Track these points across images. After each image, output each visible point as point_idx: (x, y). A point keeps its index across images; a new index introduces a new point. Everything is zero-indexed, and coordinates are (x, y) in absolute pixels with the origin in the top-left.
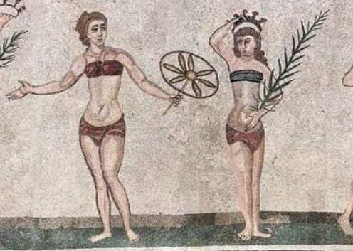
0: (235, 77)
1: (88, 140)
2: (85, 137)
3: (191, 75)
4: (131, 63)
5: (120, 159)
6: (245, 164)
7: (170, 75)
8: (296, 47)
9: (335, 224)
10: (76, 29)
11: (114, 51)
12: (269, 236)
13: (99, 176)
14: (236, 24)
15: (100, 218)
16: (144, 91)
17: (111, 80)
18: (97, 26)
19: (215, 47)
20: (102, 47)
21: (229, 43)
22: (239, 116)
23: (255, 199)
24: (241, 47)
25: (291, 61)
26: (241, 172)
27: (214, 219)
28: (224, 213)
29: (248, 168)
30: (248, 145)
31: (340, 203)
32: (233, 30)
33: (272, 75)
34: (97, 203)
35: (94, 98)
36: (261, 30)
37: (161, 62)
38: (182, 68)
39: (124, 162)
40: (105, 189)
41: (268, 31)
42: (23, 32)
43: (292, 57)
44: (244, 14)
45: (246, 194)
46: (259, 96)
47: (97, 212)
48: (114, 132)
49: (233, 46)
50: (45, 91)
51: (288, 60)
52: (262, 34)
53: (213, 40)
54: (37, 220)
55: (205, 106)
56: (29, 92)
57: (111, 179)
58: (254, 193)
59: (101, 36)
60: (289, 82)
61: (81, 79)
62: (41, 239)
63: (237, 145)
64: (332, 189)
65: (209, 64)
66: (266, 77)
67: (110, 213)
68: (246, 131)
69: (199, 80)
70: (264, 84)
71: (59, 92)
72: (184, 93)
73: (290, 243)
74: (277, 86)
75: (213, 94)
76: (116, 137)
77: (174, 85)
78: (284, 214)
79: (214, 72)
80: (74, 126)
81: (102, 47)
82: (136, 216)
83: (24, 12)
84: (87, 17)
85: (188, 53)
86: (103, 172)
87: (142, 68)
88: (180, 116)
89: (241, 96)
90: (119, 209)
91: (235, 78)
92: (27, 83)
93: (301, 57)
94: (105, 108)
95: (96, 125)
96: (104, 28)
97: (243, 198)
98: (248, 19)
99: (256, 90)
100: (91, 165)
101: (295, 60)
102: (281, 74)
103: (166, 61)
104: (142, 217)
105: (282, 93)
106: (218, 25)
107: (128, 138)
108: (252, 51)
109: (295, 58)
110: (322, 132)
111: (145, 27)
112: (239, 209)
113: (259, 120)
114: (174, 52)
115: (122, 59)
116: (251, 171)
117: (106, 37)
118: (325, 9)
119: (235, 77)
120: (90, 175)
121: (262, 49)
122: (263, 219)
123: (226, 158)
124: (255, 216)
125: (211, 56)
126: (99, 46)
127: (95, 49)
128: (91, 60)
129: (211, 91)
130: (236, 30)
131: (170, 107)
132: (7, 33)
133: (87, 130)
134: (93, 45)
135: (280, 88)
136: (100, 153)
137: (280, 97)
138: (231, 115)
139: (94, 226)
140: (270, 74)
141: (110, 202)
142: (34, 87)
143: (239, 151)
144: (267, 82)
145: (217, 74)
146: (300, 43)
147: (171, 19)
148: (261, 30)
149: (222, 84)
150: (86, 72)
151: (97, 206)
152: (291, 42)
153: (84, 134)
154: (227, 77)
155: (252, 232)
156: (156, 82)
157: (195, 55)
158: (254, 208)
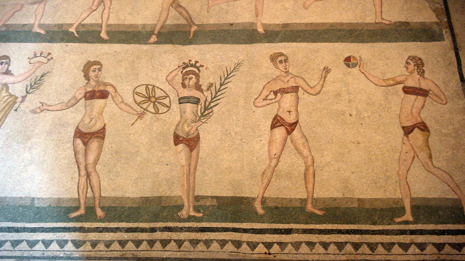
0: (182, 100)
1: (79, 141)
2: (78, 139)
3: (153, 99)
4: (114, 91)
5: (99, 155)
6: (185, 160)
7: (139, 99)
8: (222, 82)
9: (250, 207)
10: (82, 71)
11: (106, 84)
12: (201, 215)
13: (82, 167)
14: (184, 68)
15: (79, 199)
16: (121, 109)
17: (102, 101)
18: (96, 69)
19: (170, 82)
20: (97, 82)
21: (179, 79)
22: (183, 125)
23: (191, 186)
24: (186, 82)
25: (219, 91)
26: (183, 166)
27: (161, 202)
28: (168, 196)
29: (187, 163)
30: (189, 146)
31: (253, 189)
32: (182, 72)
33: (206, 100)
34: (78, 187)
35: (87, 114)
36: (200, 71)
37: (134, 91)
38: (147, 94)
39: (101, 158)
40: (85, 177)
41: (203, 73)
42: (48, 72)
43: (220, 88)
44: (189, 63)
45: (185, 182)
46: (197, 112)
47: (77, 194)
48: (98, 136)
49: (182, 81)
50: (56, 109)
51: (217, 90)
52: (201, 74)
53: (169, 78)
54: (33, 199)
55: (161, 119)
56: (45, 109)
57: (90, 170)
58: (191, 181)
59: (98, 75)
60: (218, 104)
61: (81, 101)
62: (33, 214)
63: (181, 146)
64: (247, 179)
65: (165, 92)
66: (202, 101)
67: (86, 195)
68: (187, 136)
69: (158, 102)
70: (201, 105)
71: (64, 110)
72: (147, 111)
73: (217, 221)
74: (210, 107)
75: (167, 112)
76: (100, 140)
77: (141, 105)
78: (212, 197)
79: (168, 98)
80: (71, 131)
81: (98, 83)
82: (104, 197)
83: (51, 61)
84: (90, 64)
85: (152, 85)
86: (86, 165)
87: (121, 94)
88: (143, 126)
89: (185, 112)
90: (93, 191)
91: (182, 101)
92: (45, 103)
93: (225, 88)
94: (94, 120)
95: (86, 132)
96: (100, 70)
97: (183, 185)
98: (192, 66)
99: (196, 109)
100: (79, 159)
101: (222, 90)
102: (212, 99)
103: (138, 90)
104: (110, 198)
105: (212, 111)
106: (172, 68)
107: (107, 141)
108: (194, 84)
109: (221, 89)
110: (239, 138)
111: (126, 69)
112: (180, 194)
113: (197, 129)
114: (143, 85)
115: (109, 89)
116: (190, 165)
117: (101, 75)
118: (241, 59)
119: (182, 100)
120: (76, 166)
121: (200, 83)
122: (197, 201)
123: (173, 155)
124: (191, 198)
125: (167, 87)
126: (95, 81)
127: (93, 83)
128: (89, 89)
129: (165, 109)
130: (184, 71)
131: (136, 120)
132: (39, 73)
133: (79, 135)
134: (91, 80)
135: (211, 108)
136: (85, 150)
137: (211, 114)
138: (178, 125)
139: (74, 205)
140: (205, 99)
141: (87, 186)
142: (49, 106)
143: (181, 151)
144: (203, 104)
145: (170, 99)
146: (225, 80)
147: (143, 65)
148: (200, 71)
149: (173, 105)
150: (85, 96)
151: (78, 189)
152: (219, 79)
153: (77, 137)
154: (176, 100)
155: (189, 212)
156: (129, 104)
157: (156, 87)
158: (191, 193)
